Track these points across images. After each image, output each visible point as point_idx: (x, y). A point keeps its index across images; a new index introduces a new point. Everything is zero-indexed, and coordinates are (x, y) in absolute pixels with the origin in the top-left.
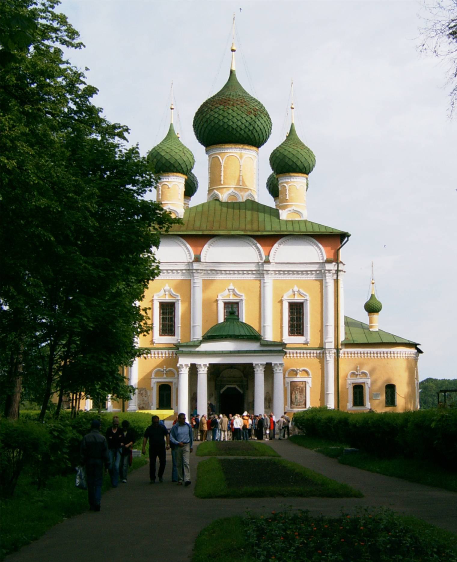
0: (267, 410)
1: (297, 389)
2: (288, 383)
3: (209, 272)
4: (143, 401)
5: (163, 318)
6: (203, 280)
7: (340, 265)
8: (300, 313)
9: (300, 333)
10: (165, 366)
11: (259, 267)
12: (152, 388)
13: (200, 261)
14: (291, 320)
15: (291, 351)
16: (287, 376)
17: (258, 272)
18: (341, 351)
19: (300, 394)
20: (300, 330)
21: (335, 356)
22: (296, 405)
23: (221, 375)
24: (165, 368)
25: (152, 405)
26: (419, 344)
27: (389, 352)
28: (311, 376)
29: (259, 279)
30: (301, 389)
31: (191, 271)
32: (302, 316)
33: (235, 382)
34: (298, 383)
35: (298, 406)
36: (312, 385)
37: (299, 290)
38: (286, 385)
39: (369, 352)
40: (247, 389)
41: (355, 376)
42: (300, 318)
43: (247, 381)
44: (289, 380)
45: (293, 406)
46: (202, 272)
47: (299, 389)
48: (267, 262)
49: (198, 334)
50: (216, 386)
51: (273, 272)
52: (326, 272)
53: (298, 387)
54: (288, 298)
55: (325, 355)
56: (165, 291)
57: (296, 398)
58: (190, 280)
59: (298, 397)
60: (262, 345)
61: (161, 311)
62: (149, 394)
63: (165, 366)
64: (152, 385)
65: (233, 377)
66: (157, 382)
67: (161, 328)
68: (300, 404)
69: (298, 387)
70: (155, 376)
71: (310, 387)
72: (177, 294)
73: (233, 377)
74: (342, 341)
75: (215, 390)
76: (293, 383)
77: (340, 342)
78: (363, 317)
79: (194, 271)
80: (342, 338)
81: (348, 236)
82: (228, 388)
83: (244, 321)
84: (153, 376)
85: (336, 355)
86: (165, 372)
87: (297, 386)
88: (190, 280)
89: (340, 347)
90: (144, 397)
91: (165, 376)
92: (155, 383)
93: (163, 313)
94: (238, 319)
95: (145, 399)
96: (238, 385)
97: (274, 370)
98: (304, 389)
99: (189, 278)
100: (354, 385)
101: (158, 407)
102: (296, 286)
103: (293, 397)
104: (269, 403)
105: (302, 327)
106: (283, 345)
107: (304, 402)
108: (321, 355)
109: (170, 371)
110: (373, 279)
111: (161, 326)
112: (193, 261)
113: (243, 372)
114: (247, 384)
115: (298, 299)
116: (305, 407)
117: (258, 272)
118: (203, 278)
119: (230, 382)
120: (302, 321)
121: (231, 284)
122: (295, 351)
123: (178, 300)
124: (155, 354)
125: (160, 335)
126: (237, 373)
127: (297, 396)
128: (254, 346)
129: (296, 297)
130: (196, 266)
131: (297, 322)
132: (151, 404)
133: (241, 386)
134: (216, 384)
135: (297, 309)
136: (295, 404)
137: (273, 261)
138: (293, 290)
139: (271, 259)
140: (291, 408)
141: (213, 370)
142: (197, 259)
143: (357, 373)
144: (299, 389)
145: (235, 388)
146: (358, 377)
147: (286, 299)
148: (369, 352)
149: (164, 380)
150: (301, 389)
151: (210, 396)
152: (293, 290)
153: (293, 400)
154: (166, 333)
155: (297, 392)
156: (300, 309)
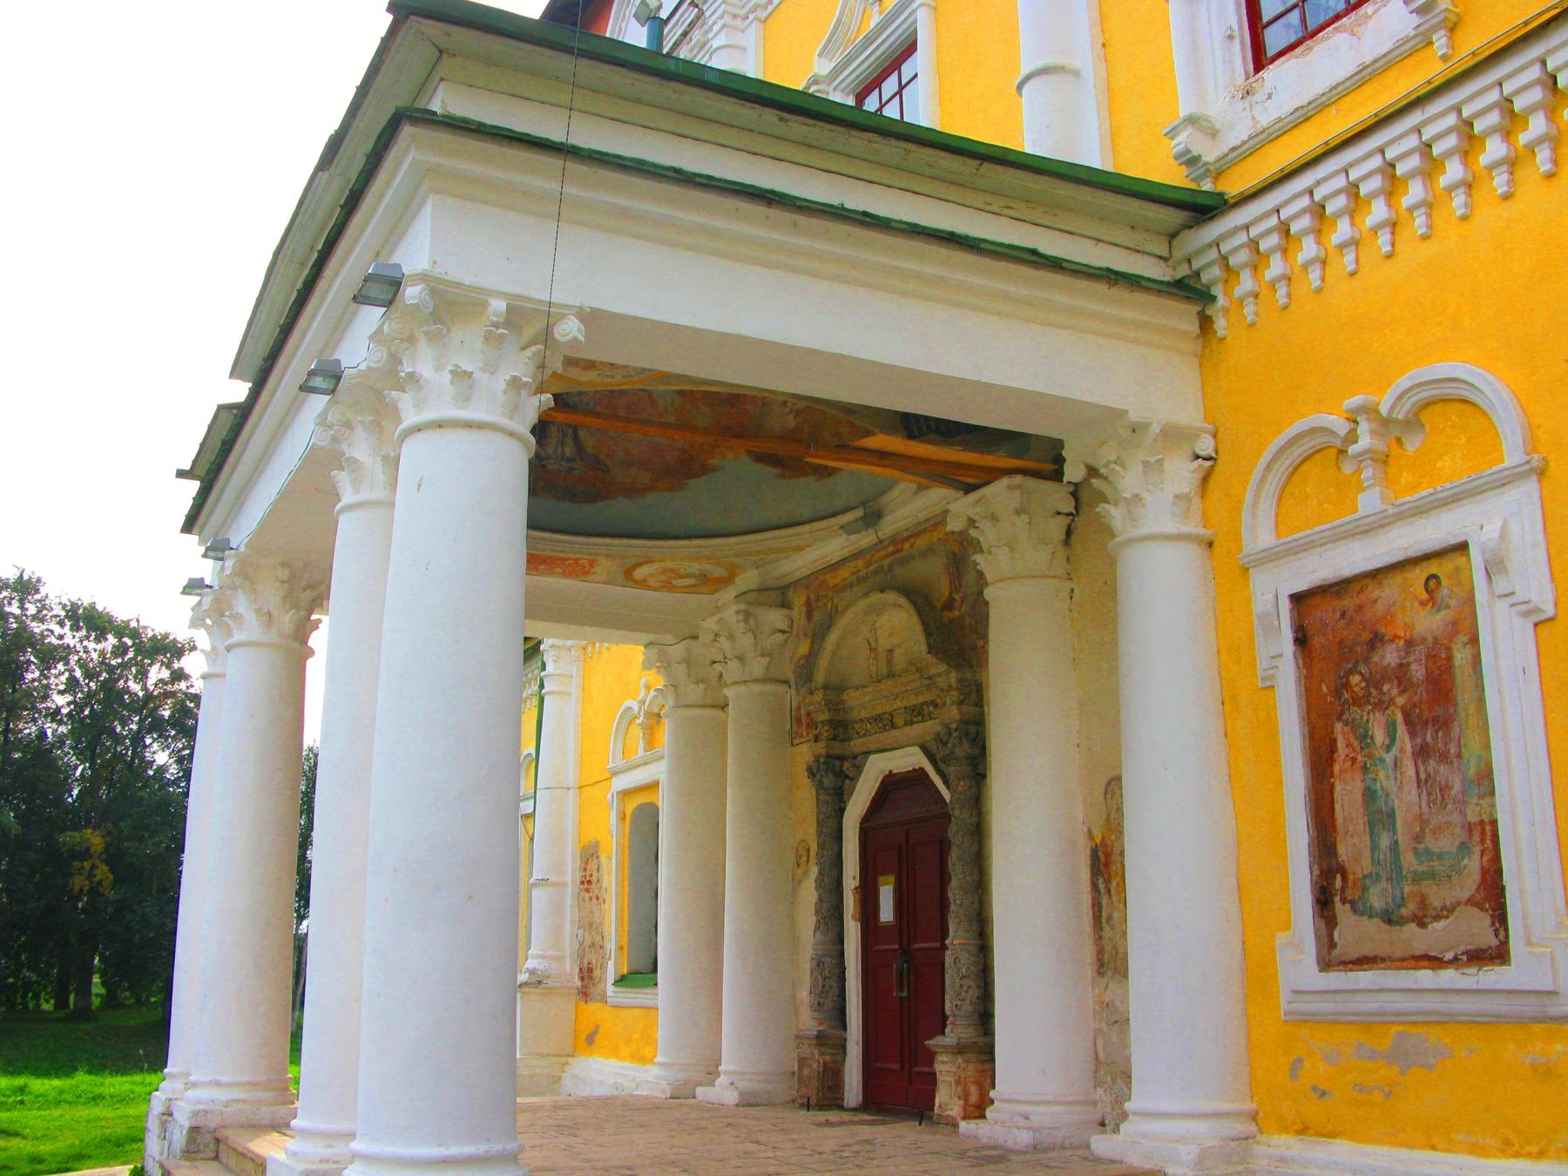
1: (1375, 681)
19: (1422, 753)
22: (1390, 919)
30: (1417, 671)
34: (1387, 592)
35: (1415, 938)
45: (1353, 931)
47: (1401, 674)
53: (1389, 656)
57: (1379, 817)
59: (1405, 799)
68: (1437, 896)
69: (1389, 656)
76: (1326, 612)
87: (1376, 640)
98: (1461, 657)
103: (1347, 795)
107: (1474, 864)
116: (1499, 955)
127: (1384, 779)
136: (1376, 899)
140: (1326, 964)
144: (1401, 674)
150: (1417, 671)
153: (1343, 851)
155: (1379, 736)
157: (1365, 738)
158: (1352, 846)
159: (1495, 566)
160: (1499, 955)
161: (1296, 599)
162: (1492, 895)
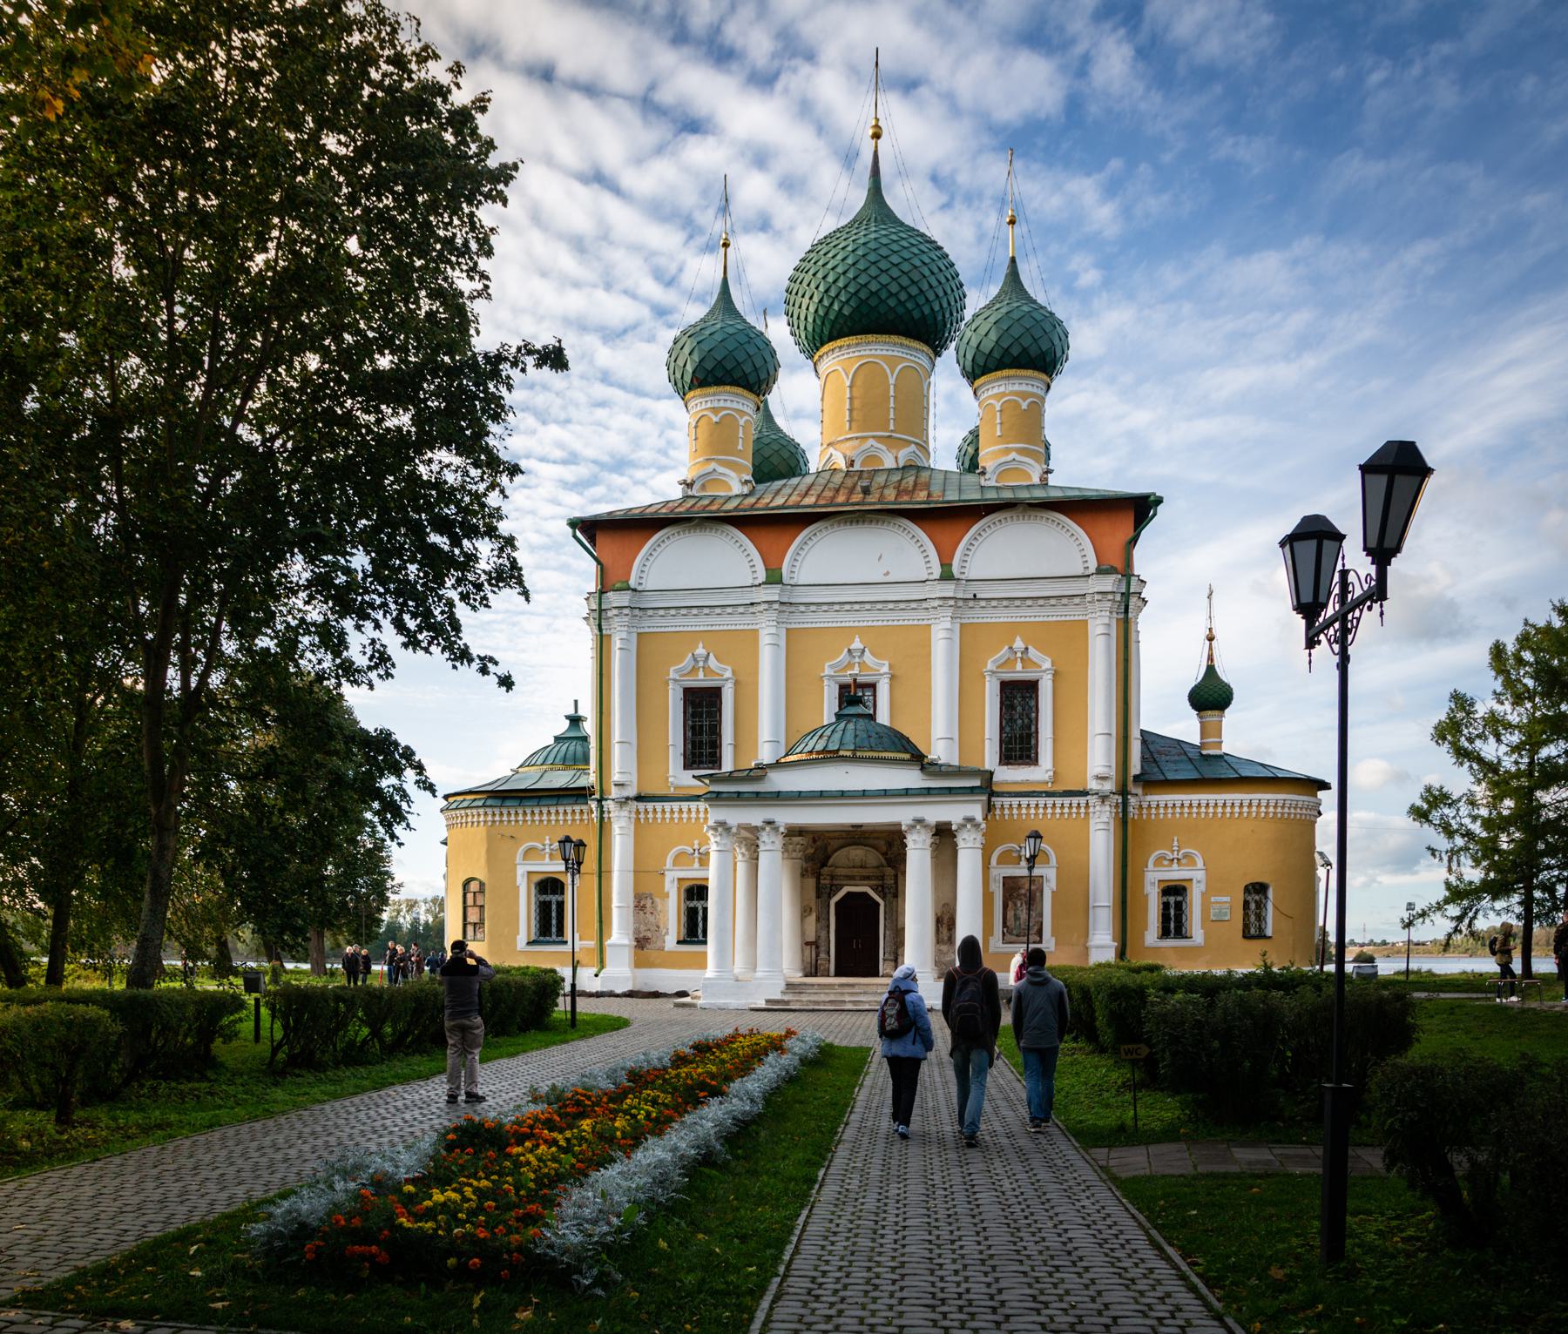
0: (944, 948)
3: (802, 608)
4: (646, 925)
10: (696, 842)
12: (667, 895)
13: (780, 582)
15: (1007, 801)
16: (994, 861)
18: (1132, 800)
20: (1029, 749)
21: (1117, 813)
23: (831, 861)
25: (667, 933)
27: (1255, 803)
28: (1053, 861)
29: (925, 622)
32: (1034, 715)
37: (1027, 649)
41: (1166, 863)
43: (896, 876)
44: (1000, 872)
46: (784, 608)
50: (818, 888)
51: (960, 603)
52: (1099, 597)
55: (1091, 810)
56: (695, 658)
61: (690, 710)
63: (696, 842)
66: (680, 880)
74: (1136, 777)
80: (1135, 768)
82: (849, 894)
89: (1132, 788)
90: (648, 915)
95: (651, 918)
102: (1018, 638)
103: (1010, 914)
105: (1033, 742)
113: (884, 854)
114: (896, 883)
115: (1019, 673)
116: (1040, 942)
118: (789, 626)
119: (852, 878)
121: (857, 639)
123: (727, 680)
127: (1019, 912)
134: (818, 883)
138: (1011, 648)
139: (955, 570)
141: (812, 851)
142: (774, 578)
145: (865, 894)
146: (1175, 866)
147: (993, 672)
148: (1204, 803)
149: (693, 873)
152: (1011, 648)
157: (1015, 905)
158: (1010, 922)
160: (1040, 942)
162: (1040, 933)
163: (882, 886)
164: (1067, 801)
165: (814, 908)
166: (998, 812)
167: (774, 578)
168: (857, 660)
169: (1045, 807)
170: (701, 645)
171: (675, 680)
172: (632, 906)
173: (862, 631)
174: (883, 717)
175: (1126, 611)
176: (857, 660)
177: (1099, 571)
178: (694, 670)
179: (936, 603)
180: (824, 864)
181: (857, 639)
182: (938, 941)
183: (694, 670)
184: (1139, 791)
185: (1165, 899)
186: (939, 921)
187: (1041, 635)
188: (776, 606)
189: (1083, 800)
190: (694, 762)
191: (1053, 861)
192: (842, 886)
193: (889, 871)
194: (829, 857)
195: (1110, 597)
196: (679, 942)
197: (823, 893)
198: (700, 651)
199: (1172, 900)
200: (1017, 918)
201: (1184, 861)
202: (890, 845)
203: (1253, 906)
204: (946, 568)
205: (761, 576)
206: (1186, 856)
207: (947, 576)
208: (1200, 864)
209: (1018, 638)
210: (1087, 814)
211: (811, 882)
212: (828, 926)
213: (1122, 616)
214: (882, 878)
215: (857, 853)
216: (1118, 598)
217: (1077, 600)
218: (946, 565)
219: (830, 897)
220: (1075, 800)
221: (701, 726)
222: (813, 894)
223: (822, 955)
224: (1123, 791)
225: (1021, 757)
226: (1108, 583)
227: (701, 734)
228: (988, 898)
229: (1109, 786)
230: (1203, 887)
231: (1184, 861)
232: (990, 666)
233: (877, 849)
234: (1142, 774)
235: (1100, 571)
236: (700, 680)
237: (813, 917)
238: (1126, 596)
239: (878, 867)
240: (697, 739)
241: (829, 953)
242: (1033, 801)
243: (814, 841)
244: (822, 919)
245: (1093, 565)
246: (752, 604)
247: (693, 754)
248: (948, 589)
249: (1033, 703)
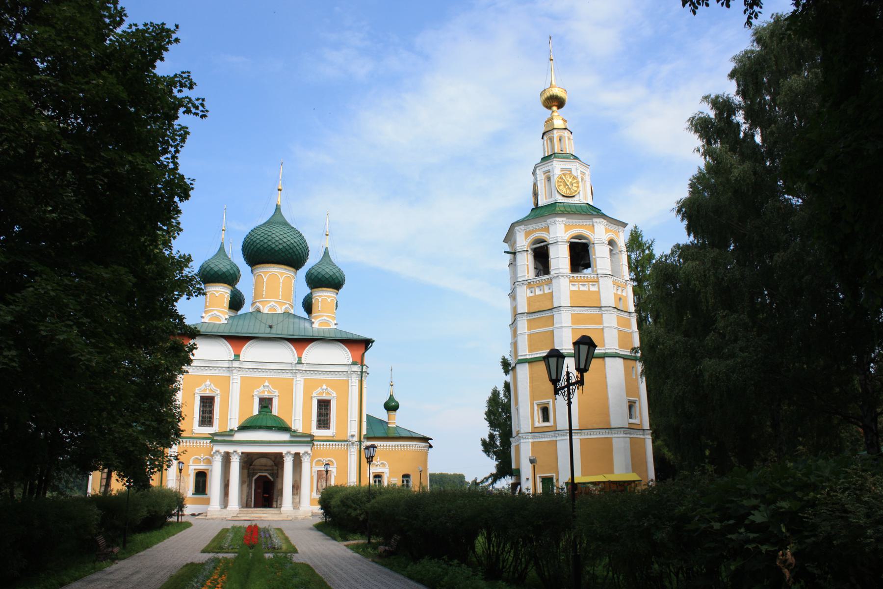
1: (323, 477)
2: (314, 472)
3: (247, 370)
5: (203, 411)
6: (241, 377)
7: (364, 367)
8: (327, 409)
9: (327, 427)
10: (202, 455)
11: (292, 367)
12: (190, 475)
14: (319, 415)
15: (319, 443)
16: (314, 465)
17: (291, 372)
20: (327, 424)
23: (254, 464)
24: (202, 457)
25: (188, 490)
26: (431, 439)
29: (292, 377)
31: (231, 369)
33: (267, 470)
36: (336, 473)
38: (313, 474)
39: (388, 445)
40: (277, 477)
42: (327, 414)
43: (278, 469)
44: (316, 469)
46: (240, 369)
48: (300, 362)
49: (235, 425)
51: (304, 372)
52: (352, 373)
54: (318, 394)
55: (348, 447)
58: (230, 377)
60: (292, 436)
61: (202, 404)
62: (186, 480)
64: (190, 472)
65: (265, 466)
66: (194, 469)
67: (201, 420)
70: (193, 463)
71: (335, 476)
72: (217, 389)
73: (265, 466)
74: (364, 435)
75: (248, 477)
76: (319, 472)
77: (362, 436)
78: (382, 415)
79: (233, 369)
80: (364, 432)
81: (373, 341)
82: (260, 476)
83: (277, 415)
84: (191, 463)
85: (359, 447)
86: (202, 460)
88: (230, 377)
91: (202, 464)
92: (192, 470)
93: (203, 406)
94: (271, 412)
96: (268, 473)
97: (302, 459)
99: (229, 375)
100: (375, 474)
101: (194, 492)
102: (324, 385)
103: (319, 484)
104: (297, 490)
105: (328, 421)
106: (311, 436)
108: (346, 447)
109: (206, 459)
110: (392, 382)
111: (201, 418)
112: (234, 360)
113: (274, 461)
115: (325, 397)
117: (291, 372)
119: (261, 470)
120: (329, 416)
121: (267, 382)
122: (322, 443)
123: (217, 394)
124: (193, 443)
125: (199, 426)
126: (270, 462)
127: (322, 484)
128: (285, 437)
129: (324, 395)
130: (236, 364)
131: (324, 416)
132: (187, 490)
133: (272, 475)
134: (248, 472)
135: (325, 405)
137: (305, 362)
138: (321, 388)
141: (246, 459)
143: (377, 464)
145: (266, 476)
147: (315, 396)
148: (388, 445)
149: (201, 467)
151: (242, 482)
152: (321, 388)
153: (319, 488)
154: (205, 424)
156: (327, 406)
158: (319, 488)
159: (333, 472)
161: (318, 471)
163: (273, 473)
164: (340, 443)
165: (246, 481)
166: (315, 446)
167: (237, 356)
168: (266, 389)
169: (332, 445)
170: (208, 380)
171: (197, 393)
172: (175, 479)
173: (269, 379)
174: (275, 411)
175: (362, 378)
176: (266, 389)
177: (354, 363)
178: (205, 390)
179: (294, 371)
180: (251, 465)
181: (267, 382)
182: (293, 494)
183: (205, 390)
184: (366, 440)
185: (375, 479)
186: (293, 486)
187: (330, 384)
188: (237, 369)
189: (346, 443)
190: (202, 424)
191: (335, 465)
192: (257, 473)
193: (275, 468)
194: (253, 462)
195: (356, 373)
196: (193, 494)
197: (250, 475)
198: (208, 382)
199: (377, 479)
200: (322, 486)
201: (381, 466)
202: (276, 458)
203: (405, 482)
204: (299, 359)
205: (233, 357)
206: (382, 463)
207: (300, 362)
208: (387, 467)
209: (324, 385)
210: (347, 448)
211: (246, 471)
212: (252, 488)
213: (360, 379)
214: (273, 470)
215: (263, 461)
216: (359, 373)
217: (345, 373)
218: (300, 358)
219: (253, 477)
220: (343, 444)
221: (206, 410)
222: (246, 475)
223: (250, 499)
224: (360, 441)
225: (324, 427)
226: (357, 368)
227: (206, 413)
228: (312, 477)
229: (356, 439)
230: (388, 475)
231: (381, 466)
232: (314, 394)
233: (271, 459)
234: (366, 434)
235: (354, 363)
236: (208, 393)
237: (245, 485)
238: (362, 372)
239: (270, 466)
240: (204, 415)
241: (251, 498)
242: (328, 443)
243: (248, 456)
244: (250, 486)
245: (351, 361)
246: (229, 367)
247: (202, 421)
248: (299, 367)
249: (329, 407)
